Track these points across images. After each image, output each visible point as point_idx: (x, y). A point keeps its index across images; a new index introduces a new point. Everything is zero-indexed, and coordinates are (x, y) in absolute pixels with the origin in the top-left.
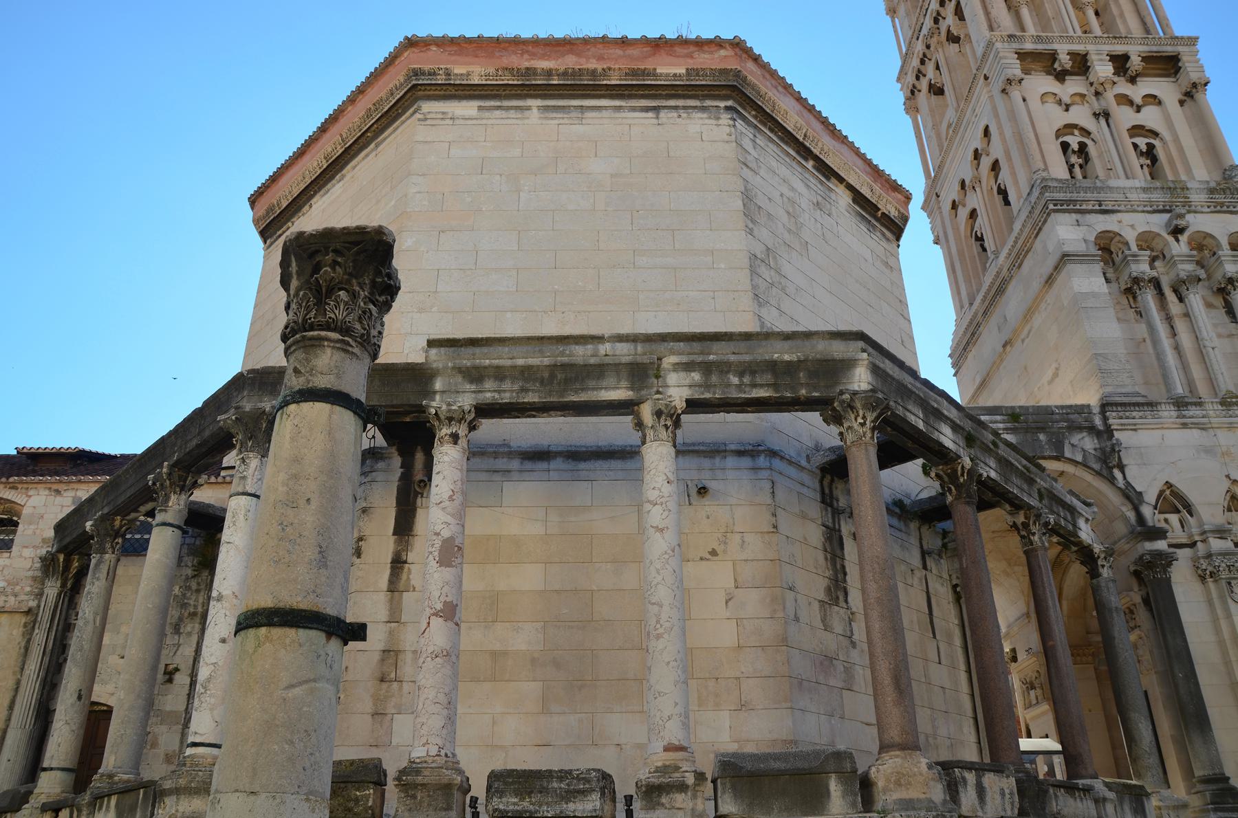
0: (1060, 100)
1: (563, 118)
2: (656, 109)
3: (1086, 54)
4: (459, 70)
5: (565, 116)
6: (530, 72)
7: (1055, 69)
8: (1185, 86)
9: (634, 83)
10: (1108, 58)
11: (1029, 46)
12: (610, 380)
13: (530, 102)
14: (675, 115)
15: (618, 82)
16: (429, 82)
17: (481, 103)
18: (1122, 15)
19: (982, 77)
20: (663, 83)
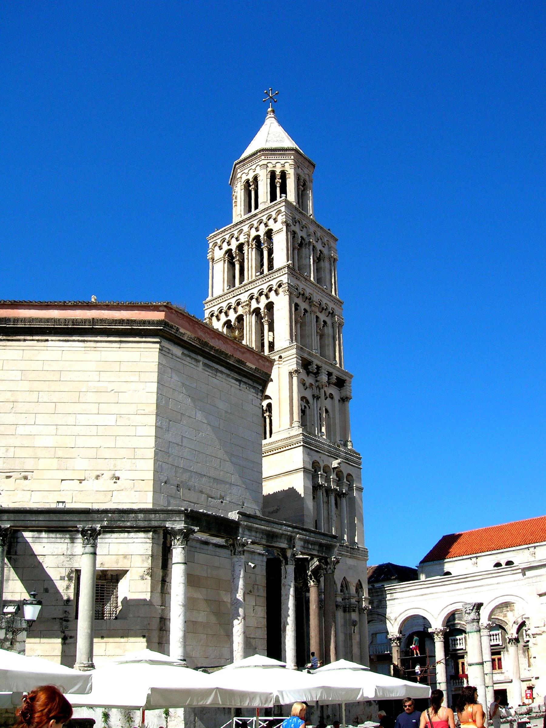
0: (305, 384)
1: (210, 372)
2: (240, 381)
3: (320, 367)
4: (182, 330)
5: (211, 371)
6: (206, 344)
7: (309, 369)
8: (344, 395)
9: (237, 365)
10: (327, 373)
11: (305, 356)
12: (283, 540)
13: (200, 358)
14: (245, 386)
15: (232, 363)
16: (168, 330)
17: (186, 352)
18: (328, 345)
19: (279, 355)
20: (246, 370)
